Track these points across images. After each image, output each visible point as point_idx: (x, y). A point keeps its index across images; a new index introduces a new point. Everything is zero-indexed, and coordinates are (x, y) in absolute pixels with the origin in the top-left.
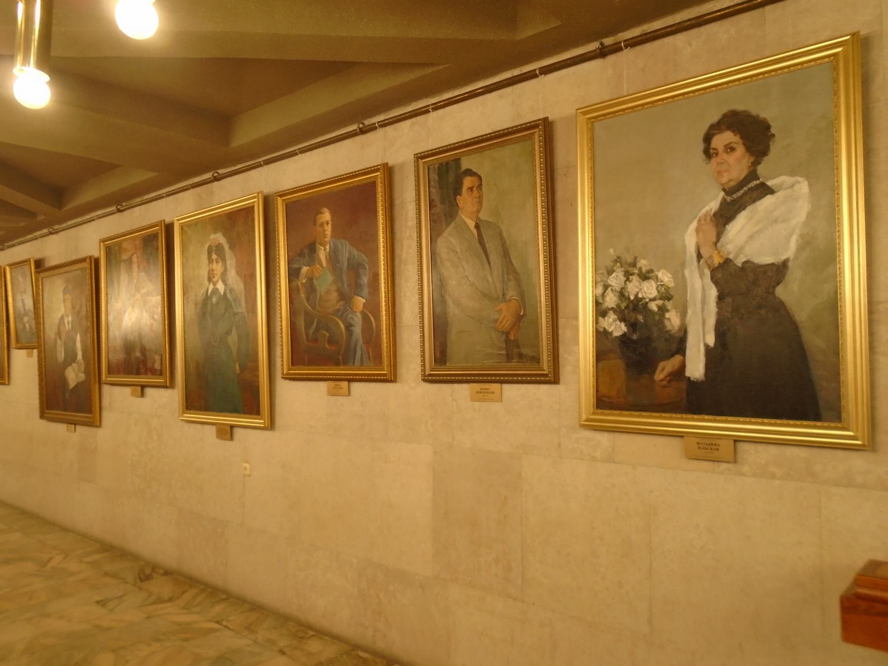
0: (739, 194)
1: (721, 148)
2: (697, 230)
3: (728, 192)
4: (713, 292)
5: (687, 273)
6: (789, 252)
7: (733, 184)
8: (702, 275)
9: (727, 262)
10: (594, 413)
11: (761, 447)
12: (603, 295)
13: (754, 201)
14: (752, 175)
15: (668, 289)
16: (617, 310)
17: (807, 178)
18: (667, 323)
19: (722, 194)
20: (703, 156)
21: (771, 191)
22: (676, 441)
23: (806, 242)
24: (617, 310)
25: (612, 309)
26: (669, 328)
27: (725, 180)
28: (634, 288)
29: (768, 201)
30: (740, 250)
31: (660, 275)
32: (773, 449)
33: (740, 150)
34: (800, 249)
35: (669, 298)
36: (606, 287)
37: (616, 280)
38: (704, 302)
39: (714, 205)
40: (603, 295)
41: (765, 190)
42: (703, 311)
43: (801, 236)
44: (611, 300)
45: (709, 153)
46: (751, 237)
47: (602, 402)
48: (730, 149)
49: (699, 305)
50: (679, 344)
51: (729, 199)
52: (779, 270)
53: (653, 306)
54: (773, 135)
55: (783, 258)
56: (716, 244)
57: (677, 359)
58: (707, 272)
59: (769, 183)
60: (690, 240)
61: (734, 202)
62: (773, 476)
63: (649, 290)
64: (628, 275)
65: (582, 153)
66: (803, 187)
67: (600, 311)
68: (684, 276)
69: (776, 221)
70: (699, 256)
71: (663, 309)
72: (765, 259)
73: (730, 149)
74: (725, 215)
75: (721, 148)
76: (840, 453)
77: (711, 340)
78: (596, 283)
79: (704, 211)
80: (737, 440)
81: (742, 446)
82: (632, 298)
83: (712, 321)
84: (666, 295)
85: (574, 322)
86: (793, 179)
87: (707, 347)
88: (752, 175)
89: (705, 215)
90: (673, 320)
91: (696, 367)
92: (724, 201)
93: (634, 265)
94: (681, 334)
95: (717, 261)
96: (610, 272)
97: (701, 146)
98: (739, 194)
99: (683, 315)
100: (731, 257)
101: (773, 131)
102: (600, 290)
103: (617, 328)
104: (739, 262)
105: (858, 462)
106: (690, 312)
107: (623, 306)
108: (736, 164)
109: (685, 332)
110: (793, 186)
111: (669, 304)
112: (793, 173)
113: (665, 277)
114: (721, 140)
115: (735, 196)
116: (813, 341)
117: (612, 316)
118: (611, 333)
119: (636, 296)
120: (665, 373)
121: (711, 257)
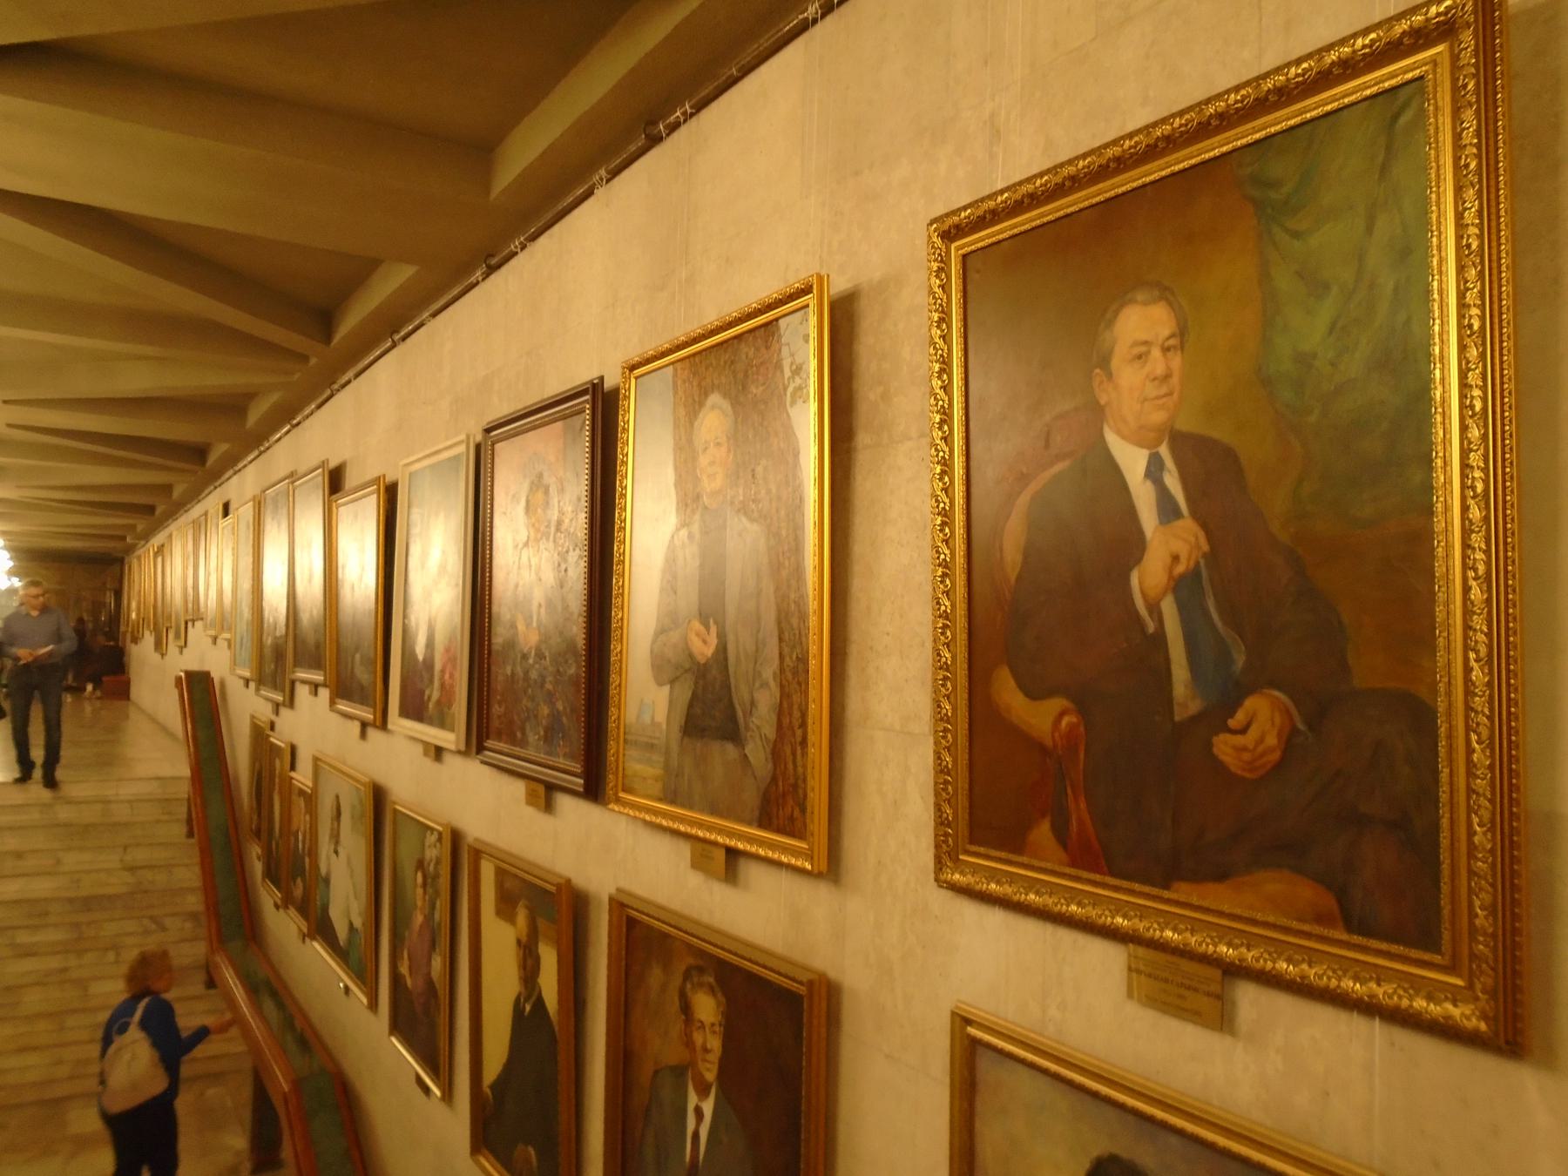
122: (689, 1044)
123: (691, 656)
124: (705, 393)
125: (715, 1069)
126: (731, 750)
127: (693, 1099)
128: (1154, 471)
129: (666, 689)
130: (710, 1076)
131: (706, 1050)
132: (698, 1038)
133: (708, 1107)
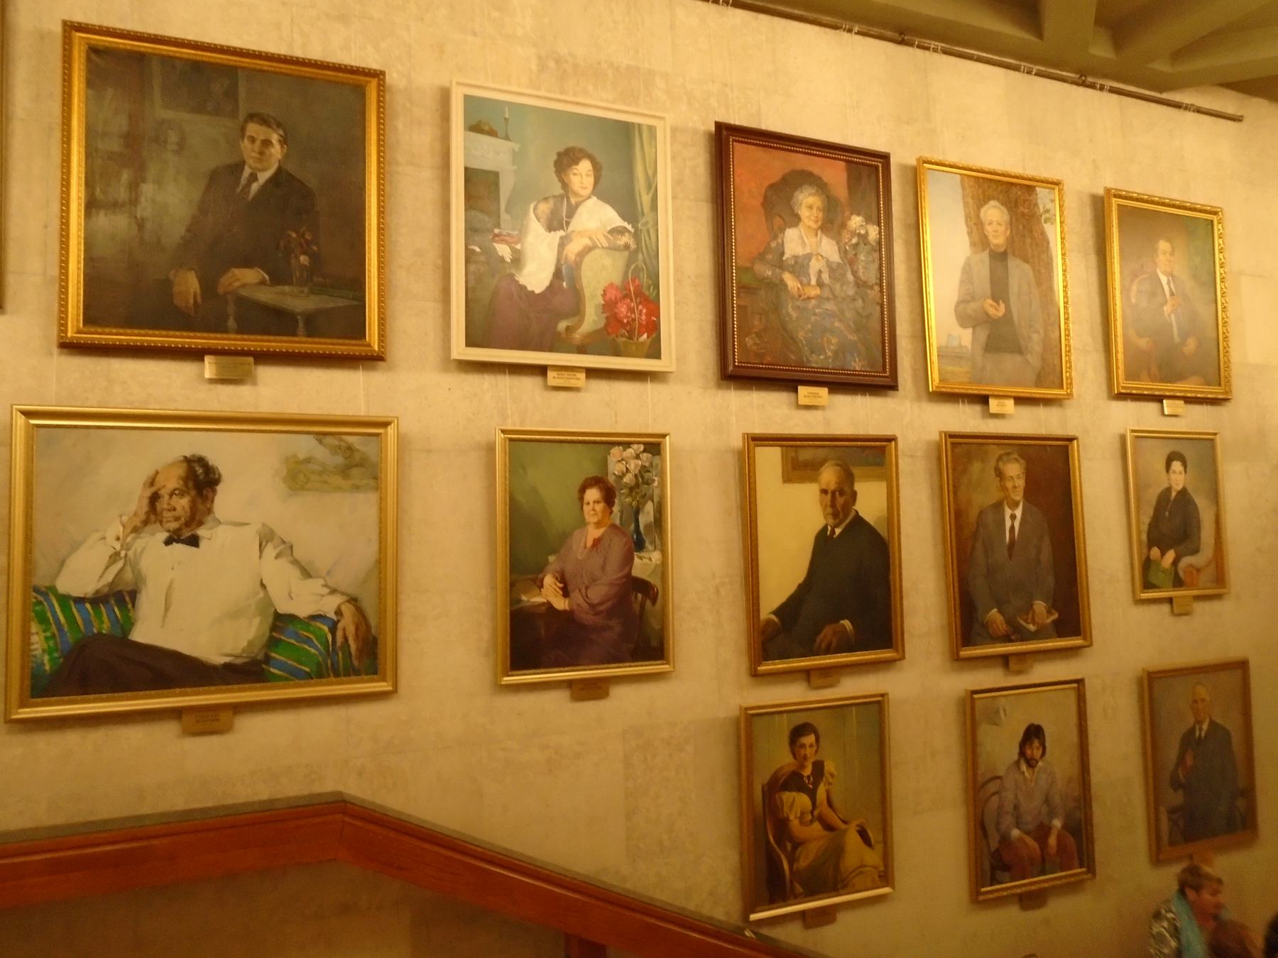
122: (1004, 488)
123: (987, 314)
124: (989, 198)
125: (1021, 494)
126: (1018, 358)
127: (1008, 512)
128: (1168, 283)
129: (970, 331)
130: (1018, 496)
131: (1015, 487)
132: (1009, 485)
133: (1019, 512)
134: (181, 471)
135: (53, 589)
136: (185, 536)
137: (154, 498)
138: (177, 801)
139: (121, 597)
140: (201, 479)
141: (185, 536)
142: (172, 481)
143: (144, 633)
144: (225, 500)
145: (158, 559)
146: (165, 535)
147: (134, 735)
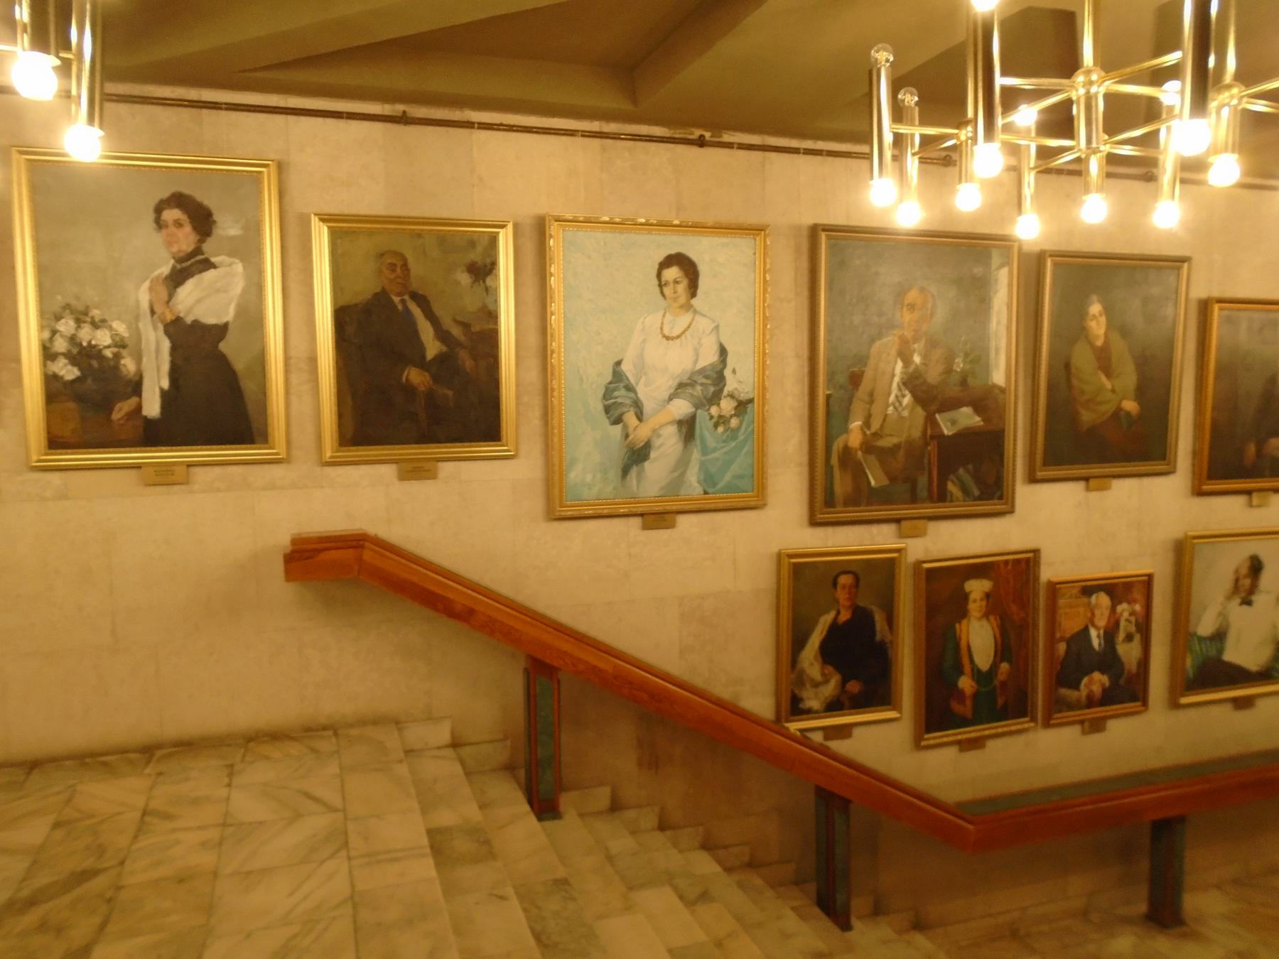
0: (189, 263)
1: (170, 222)
2: (151, 289)
3: (180, 260)
4: (166, 344)
5: (141, 325)
6: (229, 316)
7: (182, 254)
8: (155, 328)
9: (178, 320)
10: (47, 454)
11: (208, 469)
12: (51, 339)
13: (201, 272)
14: (198, 251)
15: (122, 338)
16: (68, 355)
17: (242, 261)
18: (123, 369)
19: (172, 261)
20: (154, 225)
21: (213, 266)
22: (133, 472)
23: (241, 311)
24: (68, 355)
25: (63, 354)
26: (125, 372)
27: (175, 249)
28: (85, 334)
29: (210, 275)
30: (189, 311)
31: (115, 325)
32: (217, 470)
33: (188, 228)
34: (238, 314)
35: (124, 347)
36: (54, 332)
37: (66, 326)
38: (158, 351)
39: (165, 270)
40: (51, 339)
41: (208, 265)
42: (157, 358)
43: (238, 305)
44: (60, 345)
45: (159, 224)
46: (199, 301)
47: (55, 443)
48: (178, 224)
49: (153, 355)
50: (136, 387)
51: (179, 266)
52: (222, 330)
53: (108, 353)
54: (215, 222)
55: (224, 320)
56: (168, 302)
57: (134, 400)
58: (161, 327)
59: (213, 260)
60: (144, 297)
61: (183, 270)
62: (218, 490)
63: (103, 338)
64: (79, 322)
65: (20, 194)
66: (239, 267)
67: (48, 354)
68: (138, 329)
69: (218, 291)
70: (153, 312)
71: (117, 356)
72: (211, 320)
73: (178, 224)
74: (177, 278)
75: (170, 222)
76: (267, 467)
77: (165, 384)
78: (42, 328)
79: (156, 273)
80: (190, 465)
81: (192, 469)
82: (85, 344)
83: (166, 367)
84: (120, 344)
85: (13, 365)
86: (231, 260)
87: (162, 390)
88: (198, 251)
89: (157, 277)
90: (128, 365)
91: (152, 407)
92: (174, 268)
93: (86, 314)
94: (137, 378)
95: (169, 317)
96: (58, 318)
97: (151, 216)
98: (189, 263)
99: (138, 359)
100: (182, 315)
101: (215, 217)
102: (47, 335)
103: (69, 372)
104: (189, 320)
105: (277, 471)
106: (145, 360)
107: (75, 351)
108: (186, 239)
109: (141, 377)
110: (230, 265)
111: (124, 352)
112: (231, 255)
113: (121, 328)
114: (171, 215)
115: (184, 265)
116: (248, 386)
117: (62, 361)
118: (62, 377)
119: (89, 343)
120: (122, 413)
121: (163, 313)
134: (1248, 564)
135: (1195, 634)
136: (1247, 602)
137: (1237, 580)
138: (1232, 749)
139: (1219, 636)
140: (1256, 567)
141: (1247, 602)
142: (1244, 571)
143: (1229, 656)
144: (1266, 579)
145: (1237, 612)
146: (1239, 601)
147: (1215, 711)
